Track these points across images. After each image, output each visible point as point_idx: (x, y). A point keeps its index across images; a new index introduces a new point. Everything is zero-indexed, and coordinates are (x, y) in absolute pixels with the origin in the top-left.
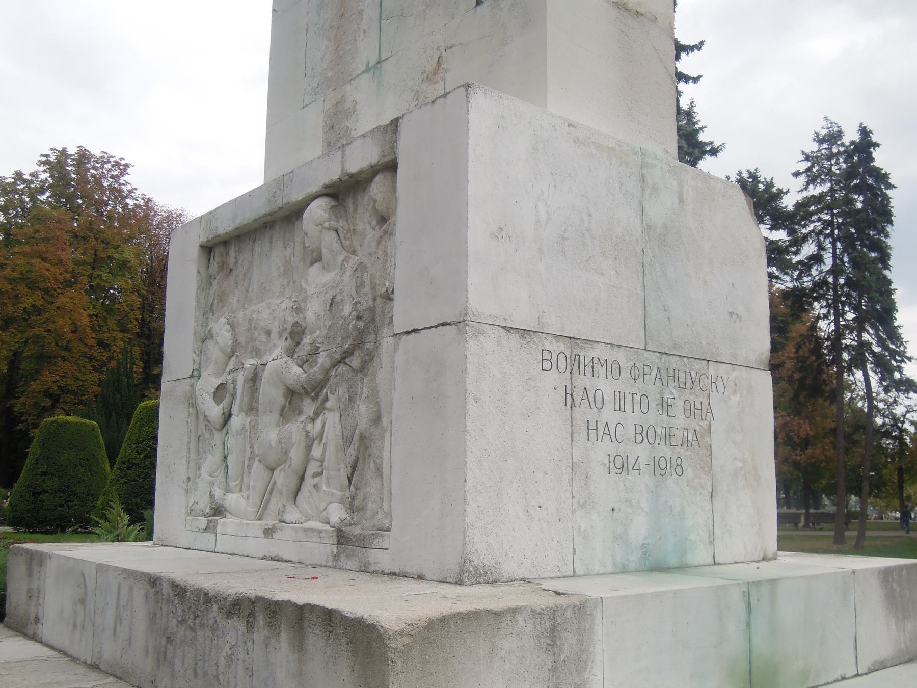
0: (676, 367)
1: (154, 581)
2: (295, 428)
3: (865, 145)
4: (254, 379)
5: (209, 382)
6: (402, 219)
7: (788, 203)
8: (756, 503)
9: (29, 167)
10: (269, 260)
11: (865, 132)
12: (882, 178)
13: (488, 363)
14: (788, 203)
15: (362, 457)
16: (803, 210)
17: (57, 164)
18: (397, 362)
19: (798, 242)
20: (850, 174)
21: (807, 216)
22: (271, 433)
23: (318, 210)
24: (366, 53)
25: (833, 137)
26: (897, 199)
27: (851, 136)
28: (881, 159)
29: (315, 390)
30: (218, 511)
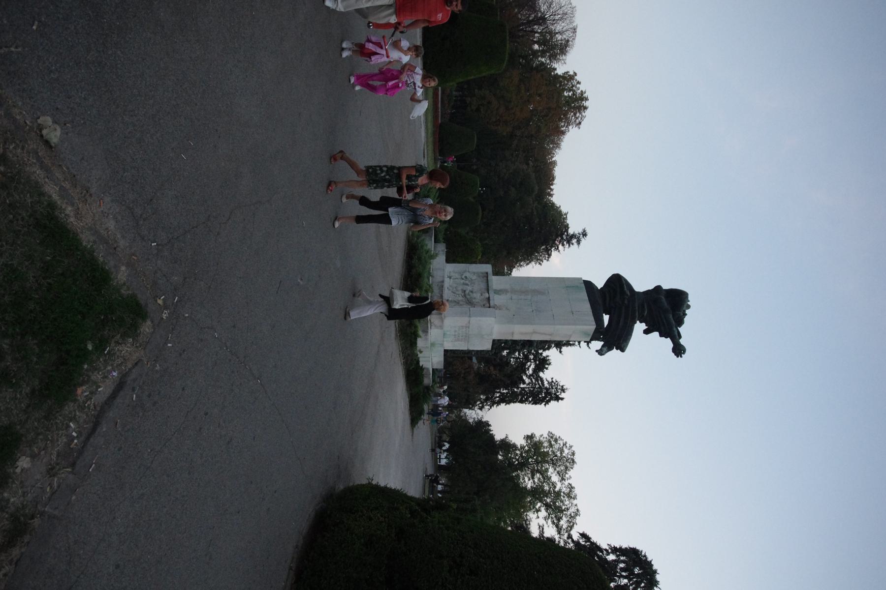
0: (467, 338)
1: (443, 282)
2: (460, 292)
3: (558, 399)
4: (467, 285)
5: (467, 274)
6: (483, 309)
7: (541, 374)
8: (449, 346)
9: (582, 87)
10: (483, 286)
11: (562, 399)
12: (547, 402)
13: (467, 319)
14: (541, 374)
15: (457, 303)
16: (538, 378)
17: (582, 98)
18: (466, 308)
19: (529, 377)
20: (550, 394)
21: (537, 380)
22: (460, 288)
23: (487, 295)
24: (514, 297)
25: (563, 390)
26: (540, 407)
27: (563, 395)
28: (553, 403)
29: (465, 296)
30: (450, 278)
